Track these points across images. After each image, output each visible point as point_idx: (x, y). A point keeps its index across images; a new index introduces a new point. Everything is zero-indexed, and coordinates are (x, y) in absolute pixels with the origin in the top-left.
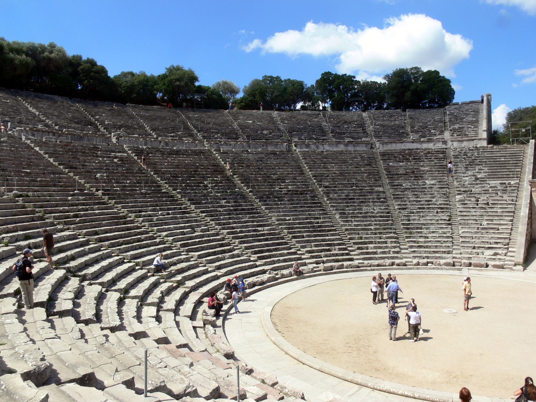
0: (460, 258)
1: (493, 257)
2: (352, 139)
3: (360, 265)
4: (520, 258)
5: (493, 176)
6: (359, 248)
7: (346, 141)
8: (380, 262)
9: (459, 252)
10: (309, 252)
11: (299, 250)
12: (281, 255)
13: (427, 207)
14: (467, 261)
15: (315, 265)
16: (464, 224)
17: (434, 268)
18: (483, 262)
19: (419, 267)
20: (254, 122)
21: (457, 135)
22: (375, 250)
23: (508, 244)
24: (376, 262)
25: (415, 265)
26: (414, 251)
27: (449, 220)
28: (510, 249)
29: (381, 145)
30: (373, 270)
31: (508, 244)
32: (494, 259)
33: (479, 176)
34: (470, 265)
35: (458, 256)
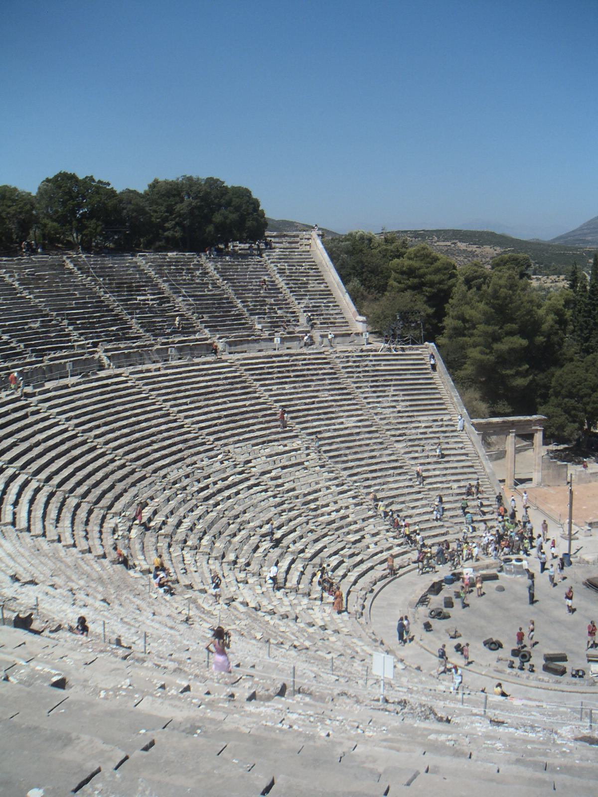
5: (418, 408)
7: (177, 340)
16: (434, 489)
21: (321, 324)
29: (227, 347)
33: (399, 409)
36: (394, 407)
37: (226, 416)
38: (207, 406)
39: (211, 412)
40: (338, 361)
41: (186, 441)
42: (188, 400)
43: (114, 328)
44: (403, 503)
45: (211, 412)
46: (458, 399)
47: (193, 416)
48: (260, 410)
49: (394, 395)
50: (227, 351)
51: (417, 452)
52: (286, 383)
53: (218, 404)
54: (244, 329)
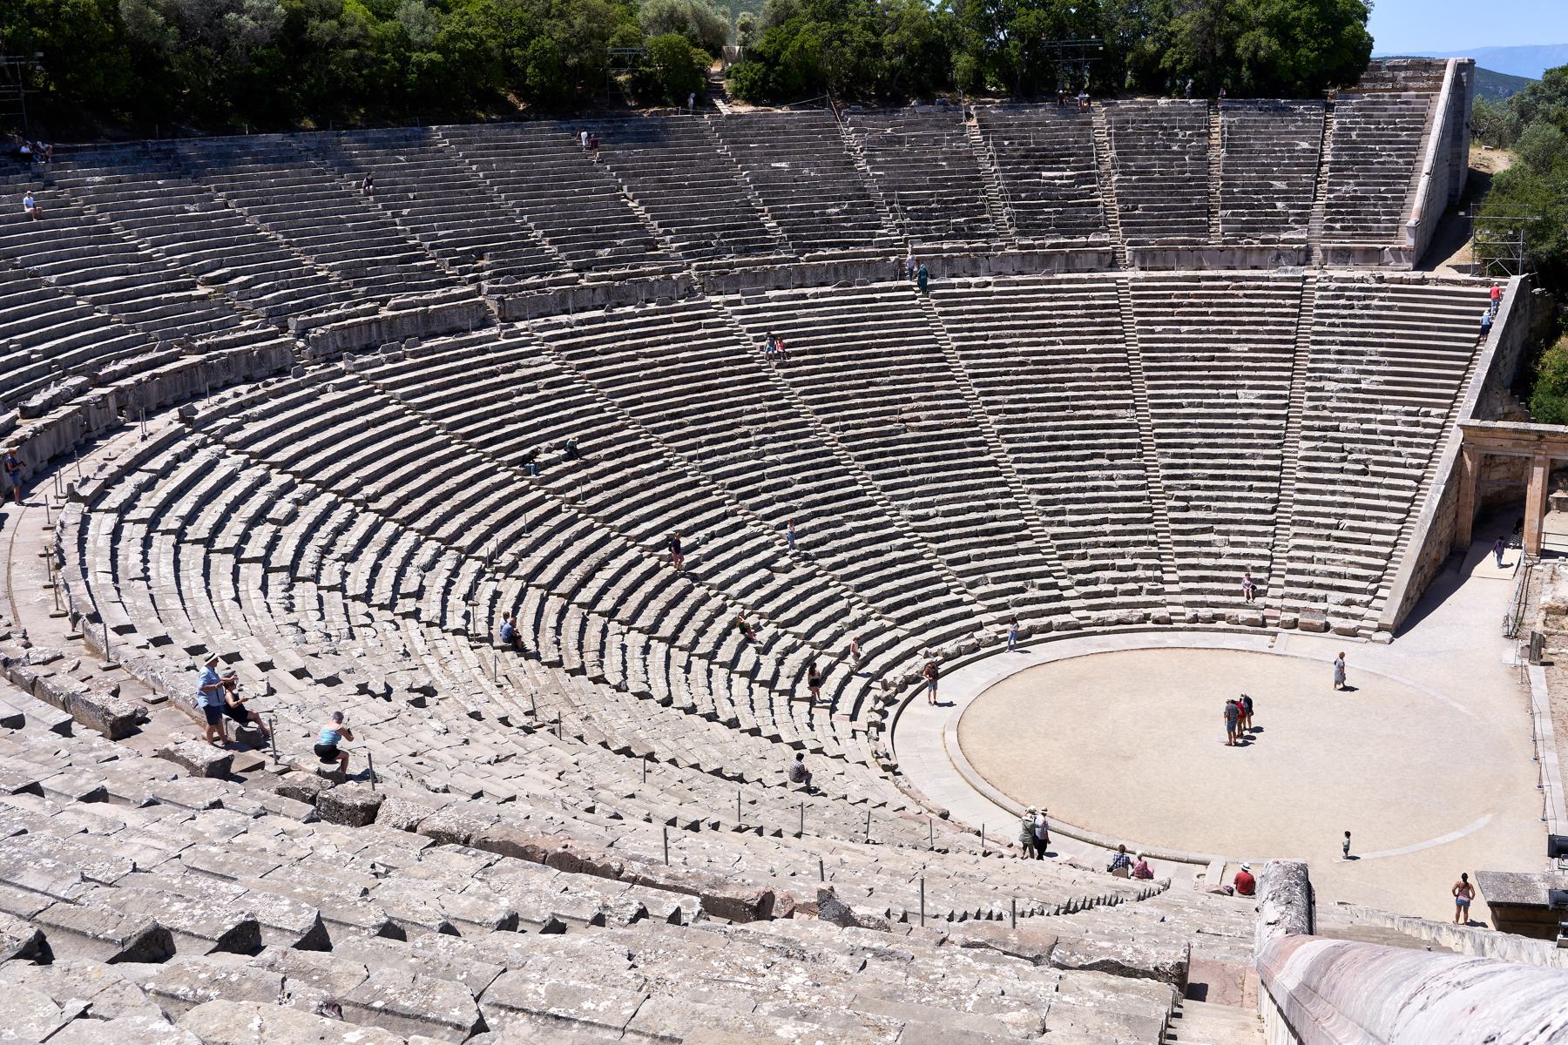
0: (1277, 608)
2: (1063, 233)
3: (1082, 622)
4: (1390, 621)
6: (1080, 583)
7: (1049, 242)
8: (1122, 613)
9: (1280, 592)
10: (984, 597)
11: (965, 592)
12: (935, 609)
13: (1230, 475)
14: (1290, 616)
15: (999, 627)
17: (1225, 630)
18: (1319, 622)
19: (1198, 625)
20: (795, 169)
21: (1343, 228)
22: (1111, 587)
23: (1379, 579)
24: (1113, 615)
25: (1189, 622)
27: (1274, 511)
28: (1381, 592)
32: (1345, 616)
33: (1363, 386)
34: (1295, 624)
35: (1277, 603)
36: (1357, 381)
37: (1036, 363)
38: (1018, 345)
39: (1016, 354)
40: (1318, 294)
41: (932, 388)
42: (990, 333)
43: (962, 220)
44: (1227, 533)
45: (1016, 354)
46: (1479, 381)
47: (979, 357)
48: (1104, 360)
50: (1137, 263)
51: (1328, 460)
52: (1190, 323)
53: (1038, 344)
54: (1188, 230)
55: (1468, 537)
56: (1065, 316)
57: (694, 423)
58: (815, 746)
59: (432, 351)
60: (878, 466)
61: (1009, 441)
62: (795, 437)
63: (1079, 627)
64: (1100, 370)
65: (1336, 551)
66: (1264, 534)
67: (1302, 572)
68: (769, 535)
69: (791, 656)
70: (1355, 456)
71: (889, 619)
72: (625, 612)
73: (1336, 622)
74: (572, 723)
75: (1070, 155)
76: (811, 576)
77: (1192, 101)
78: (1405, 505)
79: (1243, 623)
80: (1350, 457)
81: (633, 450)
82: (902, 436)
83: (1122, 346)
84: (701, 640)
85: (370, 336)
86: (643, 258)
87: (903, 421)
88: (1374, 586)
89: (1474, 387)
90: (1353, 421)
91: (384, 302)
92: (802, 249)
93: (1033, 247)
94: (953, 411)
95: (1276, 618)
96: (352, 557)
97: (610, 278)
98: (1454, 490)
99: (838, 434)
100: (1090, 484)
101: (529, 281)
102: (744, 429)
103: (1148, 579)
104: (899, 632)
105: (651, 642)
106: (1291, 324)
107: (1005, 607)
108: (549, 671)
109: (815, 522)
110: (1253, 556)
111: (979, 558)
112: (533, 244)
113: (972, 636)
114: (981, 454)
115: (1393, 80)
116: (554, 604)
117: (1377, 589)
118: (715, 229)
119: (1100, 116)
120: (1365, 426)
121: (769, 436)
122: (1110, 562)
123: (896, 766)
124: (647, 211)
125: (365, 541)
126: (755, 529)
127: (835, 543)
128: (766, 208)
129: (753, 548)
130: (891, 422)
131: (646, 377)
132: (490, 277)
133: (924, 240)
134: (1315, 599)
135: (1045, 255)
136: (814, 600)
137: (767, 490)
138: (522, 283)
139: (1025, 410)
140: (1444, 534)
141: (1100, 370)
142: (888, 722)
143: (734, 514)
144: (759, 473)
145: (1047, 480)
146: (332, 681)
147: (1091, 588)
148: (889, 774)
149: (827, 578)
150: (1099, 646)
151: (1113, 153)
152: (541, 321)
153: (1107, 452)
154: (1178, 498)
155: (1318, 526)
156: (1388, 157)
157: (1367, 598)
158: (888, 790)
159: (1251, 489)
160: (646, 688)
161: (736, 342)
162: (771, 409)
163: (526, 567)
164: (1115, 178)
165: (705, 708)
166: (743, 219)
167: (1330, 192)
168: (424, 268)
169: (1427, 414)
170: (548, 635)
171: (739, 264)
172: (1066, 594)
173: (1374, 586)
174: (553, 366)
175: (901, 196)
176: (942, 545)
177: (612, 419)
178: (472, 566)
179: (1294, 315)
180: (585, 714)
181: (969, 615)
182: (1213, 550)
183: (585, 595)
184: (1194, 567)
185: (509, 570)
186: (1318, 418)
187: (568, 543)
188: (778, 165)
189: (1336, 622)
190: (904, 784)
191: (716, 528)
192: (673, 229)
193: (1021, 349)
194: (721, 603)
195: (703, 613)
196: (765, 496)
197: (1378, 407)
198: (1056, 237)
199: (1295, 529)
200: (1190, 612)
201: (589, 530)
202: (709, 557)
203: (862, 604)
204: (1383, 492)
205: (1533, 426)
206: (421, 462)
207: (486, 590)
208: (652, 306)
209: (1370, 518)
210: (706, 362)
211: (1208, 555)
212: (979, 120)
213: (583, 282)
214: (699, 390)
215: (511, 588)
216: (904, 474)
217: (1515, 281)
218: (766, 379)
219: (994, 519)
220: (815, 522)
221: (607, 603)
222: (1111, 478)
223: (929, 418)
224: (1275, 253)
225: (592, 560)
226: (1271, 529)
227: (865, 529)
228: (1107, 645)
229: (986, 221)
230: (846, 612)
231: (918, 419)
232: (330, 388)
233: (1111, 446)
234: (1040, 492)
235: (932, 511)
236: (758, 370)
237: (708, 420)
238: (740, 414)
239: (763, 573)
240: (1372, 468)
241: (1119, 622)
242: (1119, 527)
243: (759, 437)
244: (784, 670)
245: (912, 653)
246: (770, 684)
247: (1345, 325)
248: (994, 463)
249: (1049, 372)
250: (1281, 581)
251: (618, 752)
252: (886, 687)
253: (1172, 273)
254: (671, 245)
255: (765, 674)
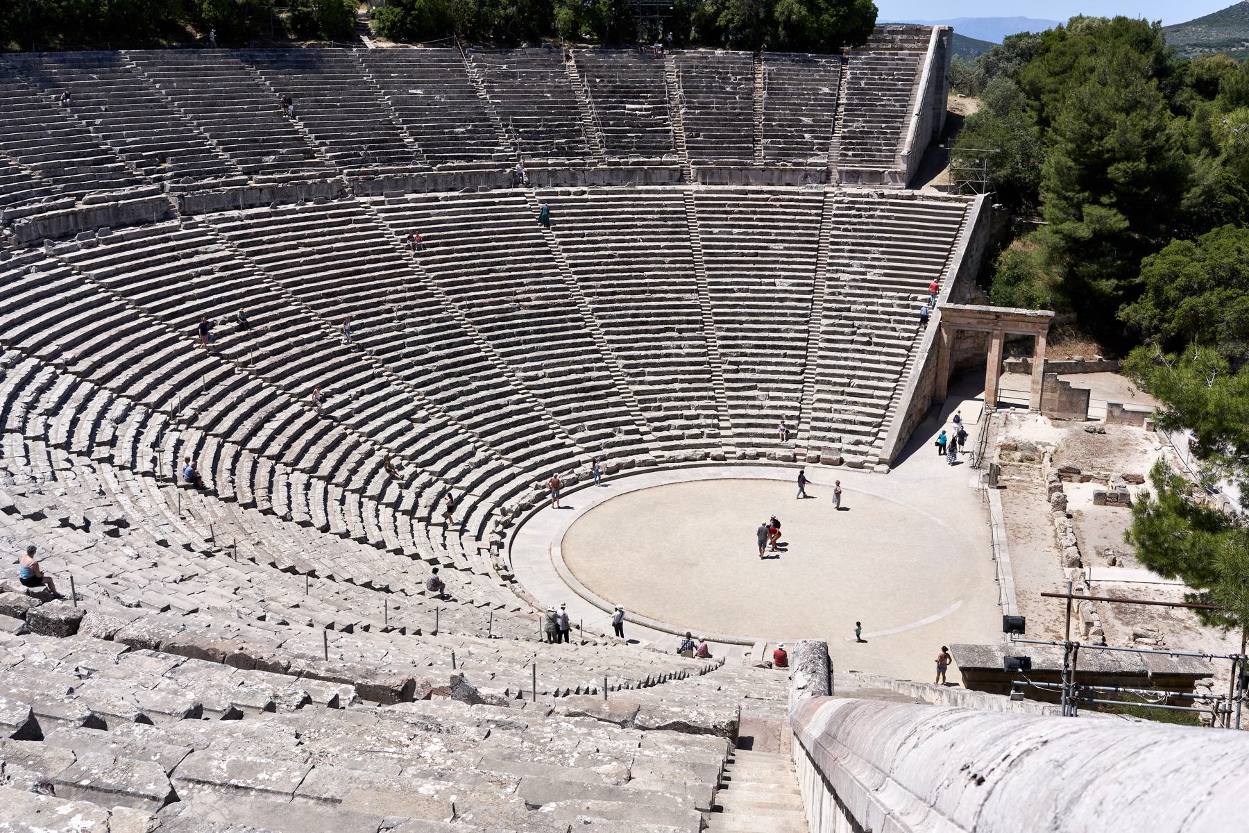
0: (804, 447)
1: (853, 448)
2: (642, 154)
3: (658, 460)
4: (887, 456)
6: (656, 429)
8: (689, 452)
9: (807, 435)
10: (582, 441)
11: (567, 437)
12: (544, 451)
14: (814, 454)
16: (823, 382)
18: (835, 457)
21: (854, 156)
22: (679, 432)
23: (880, 425)
24: (682, 454)
26: (740, 435)
27: (802, 372)
28: (881, 435)
30: (678, 468)
31: (880, 425)
32: (855, 453)
33: (868, 277)
34: (818, 459)
37: (622, 256)
38: (607, 241)
39: (606, 249)
40: (835, 206)
41: (540, 275)
42: (586, 232)
43: (563, 141)
44: (767, 390)
45: (606, 249)
47: (577, 250)
49: (874, 259)
50: (700, 179)
51: (842, 333)
52: (740, 227)
53: (623, 241)
54: (738, 154)
55: (945, 393)
56: (644, 220)
57: (346, 301)
58: (447, 561)
59: (122, 238)
60: (498, 337)
61: (601, 318)
62: (430, 313)
63: (655, 464)
64: (671, 262)
65: (848, 403)
66: (795, 391)
67: (823, 420)
68: (409, 392)
69: (427, 490)
70: (862, 331)
71: (507, 459)
72: (290, 456)
73: (848, 458)
74: (246, 548)
75: (648, 92)
76: (444, 425)
77: (741, 52)
78: (899, 368)
79: (779, 459)
80: (858, 331)
81: (295, 322)
82: (516, 313)
83: (688, 244)
84: (353, 478)
85: (68, 226)
86: (303, 165)
87: (518, 301)
88: (875, 430)
89: (949, 279)
90: (860, 304)
91: (80, 197)
92: (435, 160)
93: (619, 164)
94: (557, 293)
95: (803, 455)
96: (54, 412)
97: (274, 181)
98: (934, 358)
99: (465, 311)
100: (664, 352)
101: (205, 181)
102: (388, 306)
103: (708, 426)
104: (515, 470)
105: (312, 480)
106: (815, 228)
107: (598, 448)
108: (225, 505)
109: (446, 382)
110: (786, 408)
111: (578, 410)
112: (209, 151)
113: (573, 472)
114: (579, 328)
115: (892, 41)
116: (229, 450)
117: (878, 432)
118: (362, 142)
119: (671, 63)
120: (870, 308)
121: (409, 312)
122: (679, 412)
123: (513, 576)
124: (305, 126)
125: (64, 398)
126: (398, 388)
127: (463, 399)
128: (405, 127)
129: (396, 403)
130: (507, 302)
131: (306, 263)
132: (171, 177)
133: (533, 156)
134: (832, 440)
135: (628, 170)
136: (446, 444)
137: (407, 356)
138: (199, 183)
139: (613, 293)
140: (927, 390)
141: (671, 262)
142: (506, 541)
143: (380, 375)
144: (401, 342)
145: (630, 349)
146: (38, 516)
147: (665, 433)
148: (507, 582)
149: (457, 427)
150: (671, 478)
151: (681, 92)
152: (216, 215)
153: (677, 326)
154: (731, 363)
155: (835, 384)
156: (887, 101)
157: (871, 439)
158: (507, 596)
159: (785, 356)
160: (307, 518)
161: (381, 235)
162: (410, 290)
163: (205, 419)
164: (682, 111)
165: (357, 533)
166: (386, 135)
167: (845, 127)
168: (114, 169)
169: (915, 299)
170: (224, 476)
171: (383, 172)
172: (645, 438)
173: (875, 430)
174: (226, 253)
175: (514, 120)
176: (549, 400)
177: (277, 297)
178: (157, 420)
179: (817, 222)
180: (257, 540)
181: (571, 455)
182: (757, 403)
183: (256, 442)
184: (742, 416)
185: (190, 422)
186: (835, 301)
187: (241, 400)
188: (414, 91)
189: (848, 458)
190: (519, 590)
191: (365, 386)
192: (328, 142)
193: (610, 245)
194: (370, 447)
195: (355, 456)
196: (405, 361)
197: (879, 293)
198: (637, 157)
199: (818, 387)
200: (739, 451)
201: (258, 389)
202: (359, 410)
203: (485, 448)
204: (883, 358)
205: (992, 309)
206: (113, 331)
207: (170, 439)
208: (310, 204)
209: (873, 378)
210: (356, 251)
211: (753, 407)
212: (576, 62)
213: (252, 184)
214: (350, 274)
215: (192, 437)
216: (518, 343)
217: (980, 198)
218: (406, 265)
219: (590, 379)
220: (446, 382)
221: (274, 449)
222: (679, 347)
223: (538, 299)
224: (803, 173)
225: (262, 413)
226: (800, 386)
227: (487, 387)
228: (677, 477)
229: (582, 142)
230: (472, 454)
231: (529, 300)
232: (33, 269)
233: (680, 322)
234: (625, 358)
235: (540, 373)
236: (399, 258)
237: (358, 299)
238: (384, 294)
239: (405, 423)
240: (875, 340)
241: (686, 459)
242: (686, 385)
243: (400, 313)
244: (422, 501)
245: (525, 486)
246: (411, 513)
247: (855, 230)
248: (590, 335)
249: (632, 263)
250: (807, 427)
251: (285, 571)
252: (504, 513)
253: (726, 188)
254: (325, 155)
255: (407, 504)
